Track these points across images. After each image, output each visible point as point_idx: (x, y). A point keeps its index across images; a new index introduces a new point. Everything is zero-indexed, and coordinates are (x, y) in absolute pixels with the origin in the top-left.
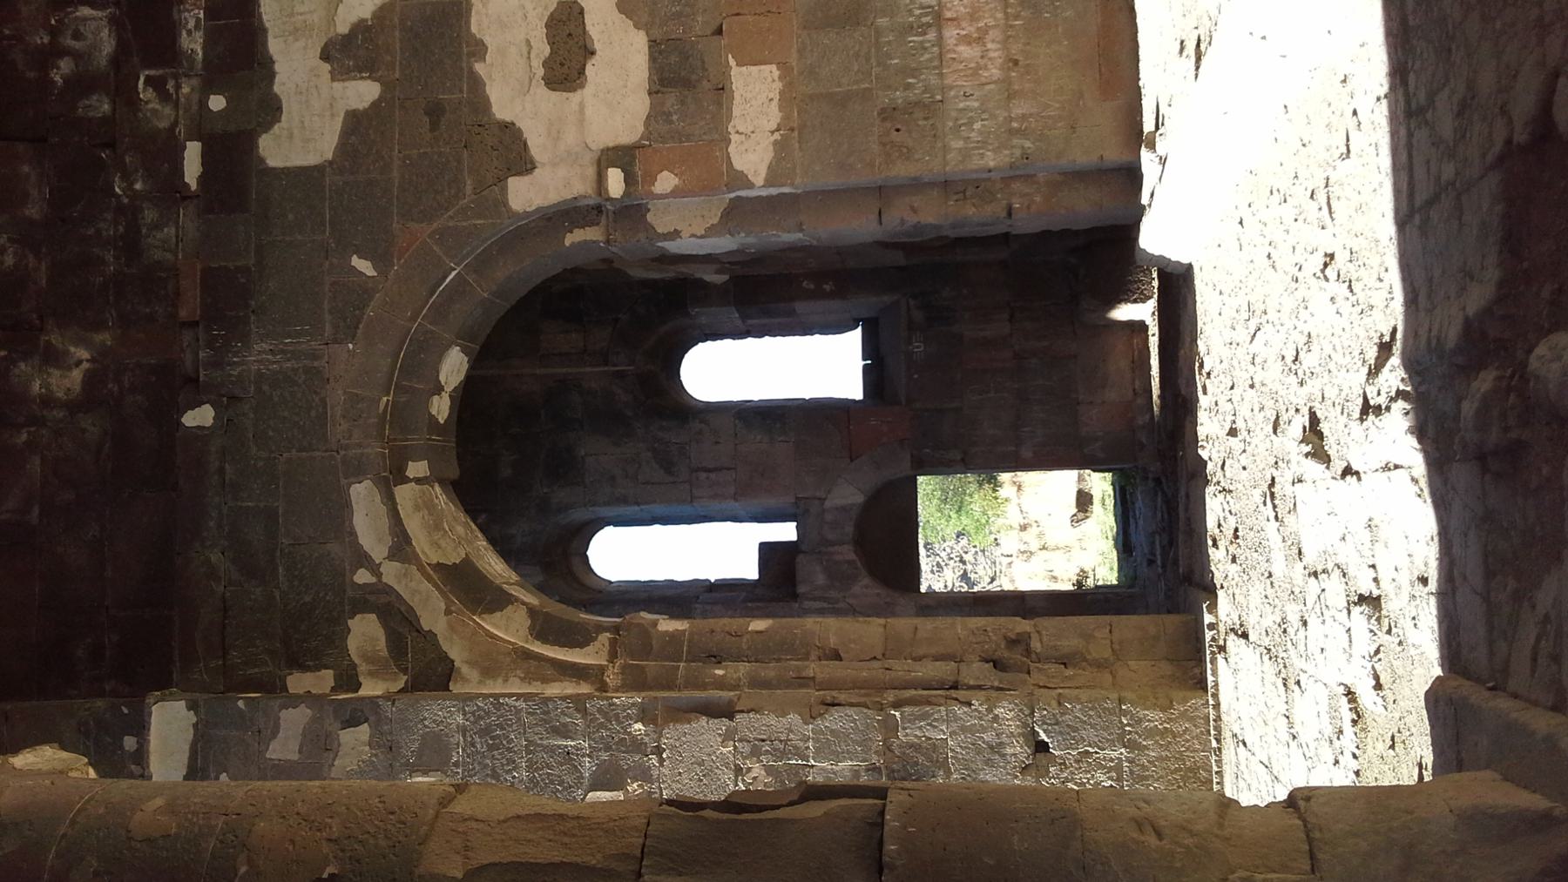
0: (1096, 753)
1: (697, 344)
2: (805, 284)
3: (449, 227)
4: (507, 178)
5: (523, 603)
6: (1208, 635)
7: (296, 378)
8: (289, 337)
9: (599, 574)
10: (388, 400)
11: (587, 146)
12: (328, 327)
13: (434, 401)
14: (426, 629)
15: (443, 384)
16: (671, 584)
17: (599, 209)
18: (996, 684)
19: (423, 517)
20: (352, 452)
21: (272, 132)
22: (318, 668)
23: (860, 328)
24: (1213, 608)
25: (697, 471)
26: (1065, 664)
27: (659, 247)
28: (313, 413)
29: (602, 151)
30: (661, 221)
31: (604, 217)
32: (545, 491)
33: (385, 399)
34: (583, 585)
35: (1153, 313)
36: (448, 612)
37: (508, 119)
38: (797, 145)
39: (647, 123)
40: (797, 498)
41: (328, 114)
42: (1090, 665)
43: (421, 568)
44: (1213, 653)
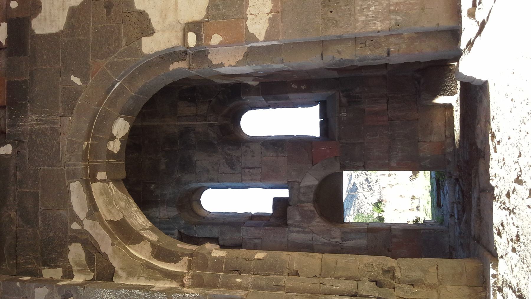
1: (248, 111)
2: (293, 86)
3: (115, 62)
4: (142, 38)
5: (149, 241)
6: (492, 280)
7: (47, 133)
8: (44, 113)
9: (205, 209)
11: (179, 22)
12: (61, 109)
13: (110, 143)
14: (103, 252)
16: (235, 215)
17: (185, 52)
19: (104, 198)
20: (71, 168)
21: (37, 17)
22: (56, 267)
23: (319, 105)
24: (495, 266)
25: (244, 169)
26: (413, 285)
27: (215, 71)
28: (54, 149)
29: (186, 24)
30: (215, 58)
31: (188, 56)
32: (179, 175)
33: (86, 143)
34: (196, 214)
35: (457, 101)
36: (113, 244)
37: (142, 9)
38: (280, 20)
39: (207, 11)
40: (288, 181)
41: (61, 9)
42: (427, 287)
43: (102, 223)
44: (494, 290)
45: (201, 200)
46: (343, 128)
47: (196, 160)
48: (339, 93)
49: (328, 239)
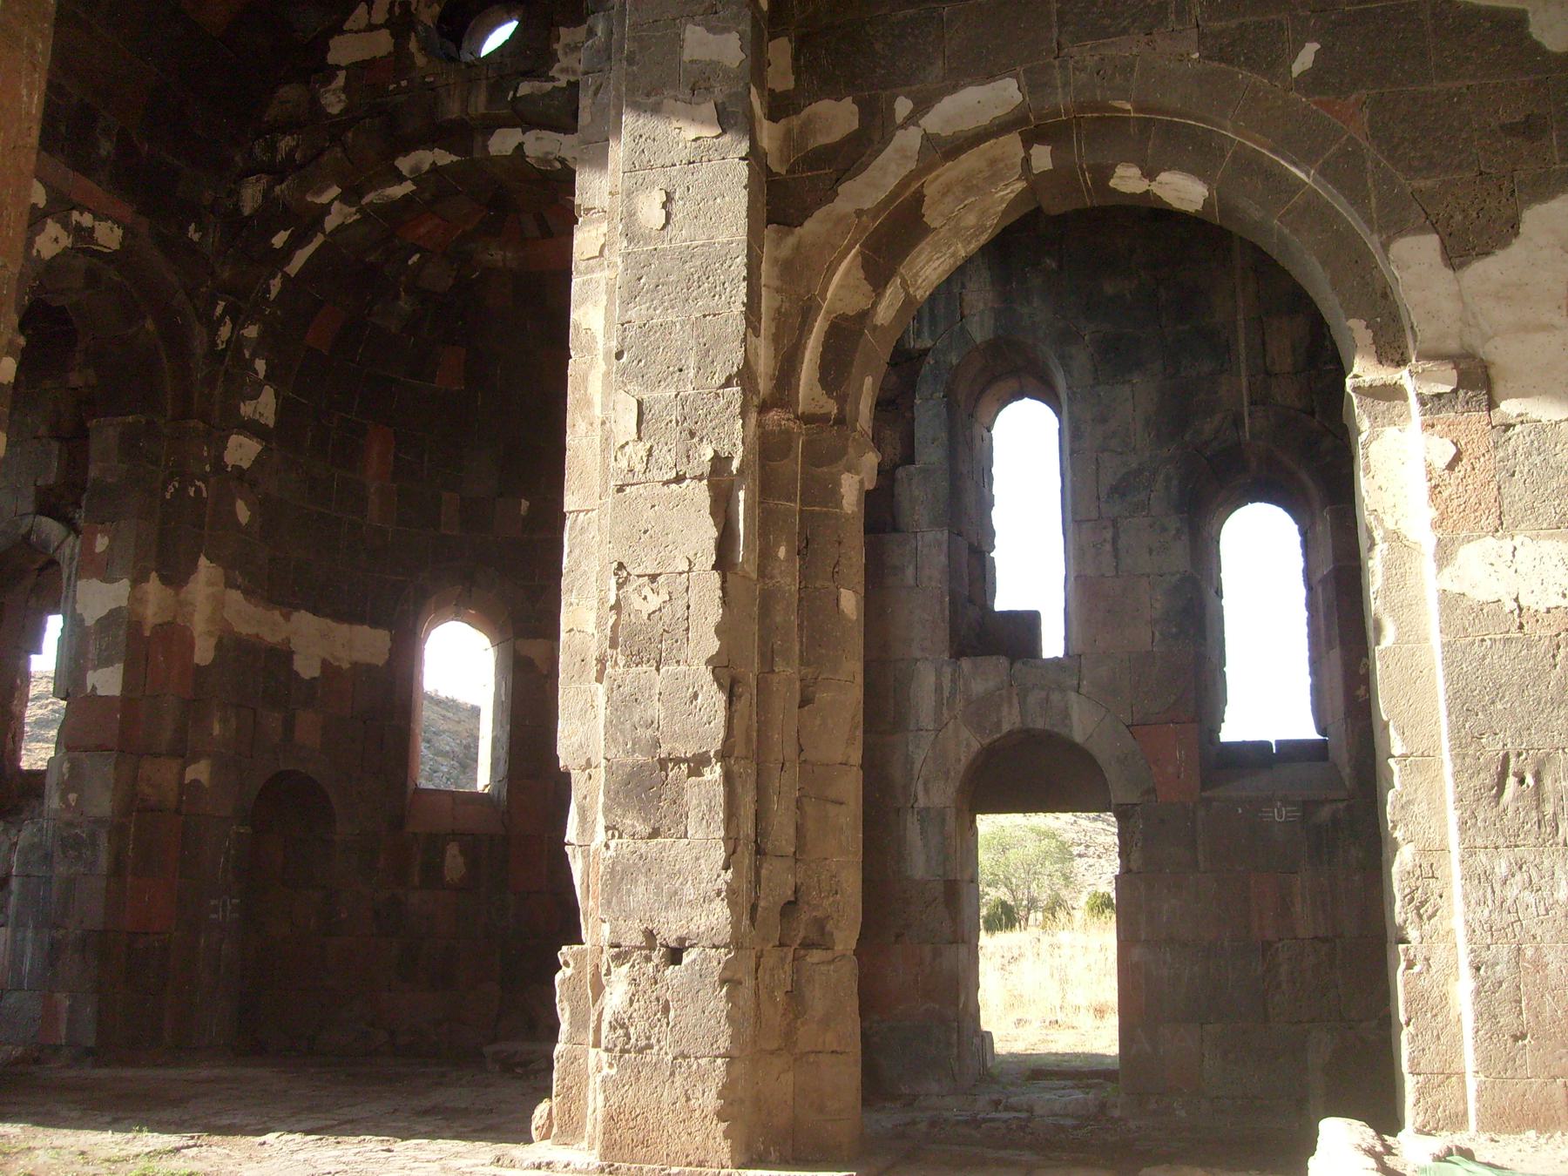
0: (668, 1024)
1: (1296, 523)
4: (1438, 233)
5: (874, 305)
10: (1129, 111)
14: (840, 189)
15: (1158, 178)
16: (986, 503)
18: (762, 903)
20: (1057, 73)
22: (797, 72)
23: (1321, 737)
25: (1114, 526)
28: (1107, 22)
33: (1128, 107)
34: (982, 391)
36: (859, 213)
42: (788, 1025)
45: (1026, 400)
46: (1240, 811)
47: (1133, 385)
48: (1344, 800)
49: (923, 773)
